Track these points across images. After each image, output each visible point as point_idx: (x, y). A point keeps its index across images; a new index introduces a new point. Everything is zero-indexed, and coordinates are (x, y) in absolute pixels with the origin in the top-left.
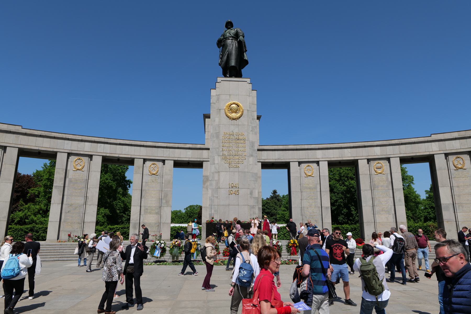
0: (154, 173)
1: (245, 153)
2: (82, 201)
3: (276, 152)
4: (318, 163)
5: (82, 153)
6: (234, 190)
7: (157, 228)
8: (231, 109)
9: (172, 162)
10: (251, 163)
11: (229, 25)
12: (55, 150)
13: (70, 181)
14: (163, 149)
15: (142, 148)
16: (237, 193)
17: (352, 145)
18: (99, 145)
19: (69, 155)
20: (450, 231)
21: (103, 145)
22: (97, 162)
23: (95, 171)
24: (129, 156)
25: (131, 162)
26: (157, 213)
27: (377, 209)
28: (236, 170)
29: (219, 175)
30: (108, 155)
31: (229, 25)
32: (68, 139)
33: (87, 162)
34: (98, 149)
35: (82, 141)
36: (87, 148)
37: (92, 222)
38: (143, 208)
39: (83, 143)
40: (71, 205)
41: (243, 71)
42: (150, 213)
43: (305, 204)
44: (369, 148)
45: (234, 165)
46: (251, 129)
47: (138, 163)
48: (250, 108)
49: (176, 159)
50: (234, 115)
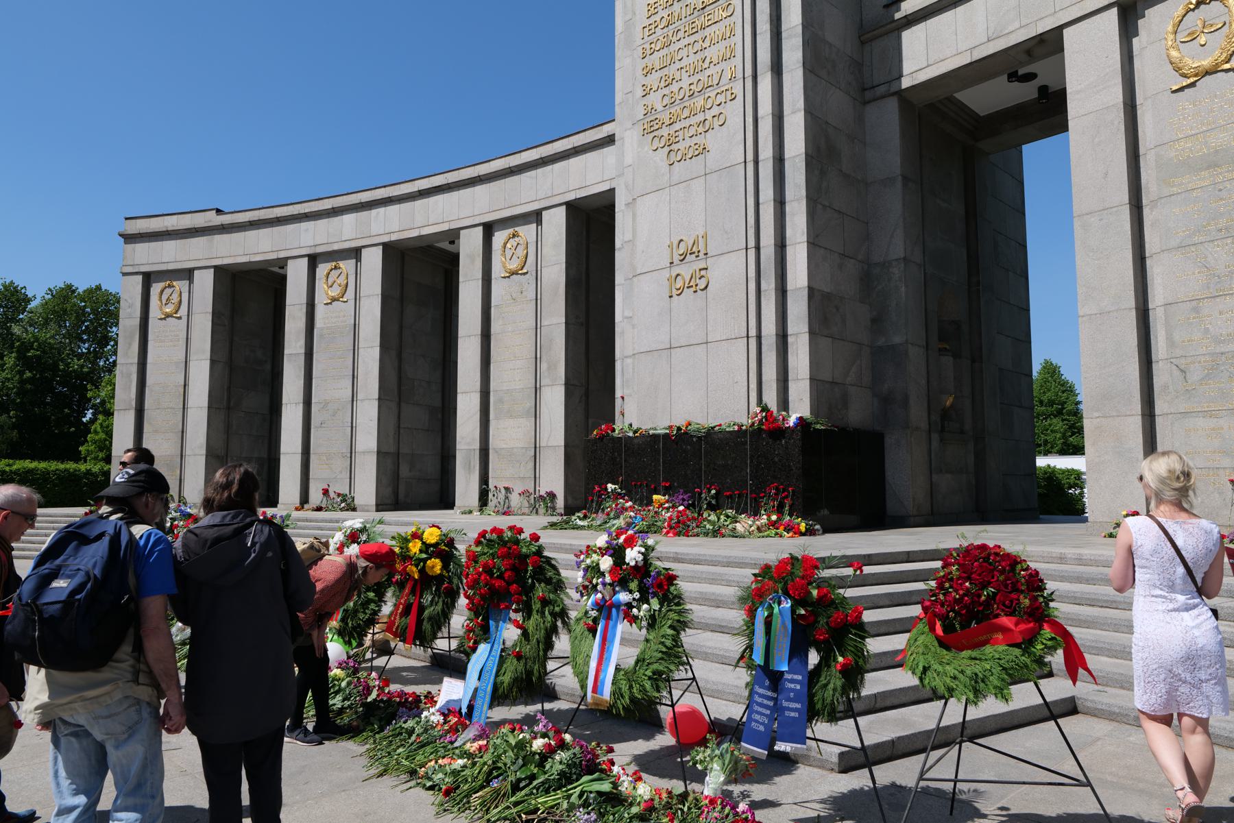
0: (513, 266)
6: (686, 271)
9: (561, 213)
14: (533, 173)
16: (698, 285)
24: (445, 227)
28: (696, 165)
29: (634, 216)
30: (394, 237)
40: (326, 403)
45: (689, 142)
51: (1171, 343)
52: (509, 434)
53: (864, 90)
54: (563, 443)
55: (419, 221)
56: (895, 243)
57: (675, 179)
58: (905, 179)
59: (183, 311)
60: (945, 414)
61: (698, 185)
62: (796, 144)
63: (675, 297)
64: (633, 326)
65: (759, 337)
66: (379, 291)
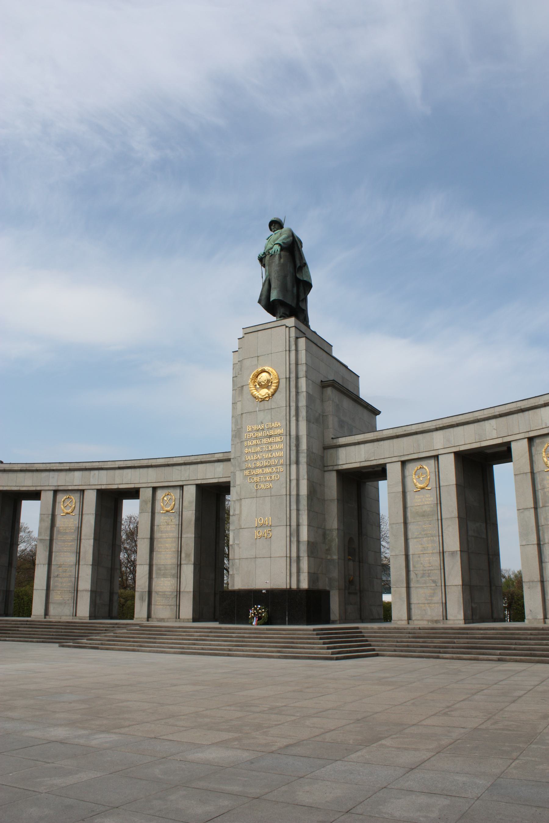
0: (169, 509)
1: (281, 461)
2: (72, 559)
3: (362, 446)
4: (436, 457)
5: (70, 488)
7: (175, 599)
8: (259, 384)
10: (294, 476)
12: (38, 488)
13: (59, 532)
15: (150, 470)
17: (497, 411)
18: (93, 472)
19: (56, 492)
21: (96, 472)
22: (91, 498)
23: (88, 514)
24: (132, 486)
25: (380, 472)
26: (173, 576)
29: (241, 506)
30: (103, 487)
32: (53, 470)
33: (78, 500)
34: (91, 479)
35: (70, 470)
36: (76, 480)
37: (86, 591)
38: (154, 568)
39: (71, 474)
40: (60, 566)
42: (164, 576)
44: (531, 412)
46: (293, 412)
47: (394, 470)
49: (199, 482)
50: (264, 392)
51: (414, 567)
52: (164, 584)
53: (324, 466)
54: (192, 590)
56: (333, 522)
57: (258, 495)
58: (338, 500)
60: (351, 582)
61: (268, 499)
62: (304, 491)
63: (258, 540)
64: (240, 548)
65: (290, 557)
66: (94, 512)
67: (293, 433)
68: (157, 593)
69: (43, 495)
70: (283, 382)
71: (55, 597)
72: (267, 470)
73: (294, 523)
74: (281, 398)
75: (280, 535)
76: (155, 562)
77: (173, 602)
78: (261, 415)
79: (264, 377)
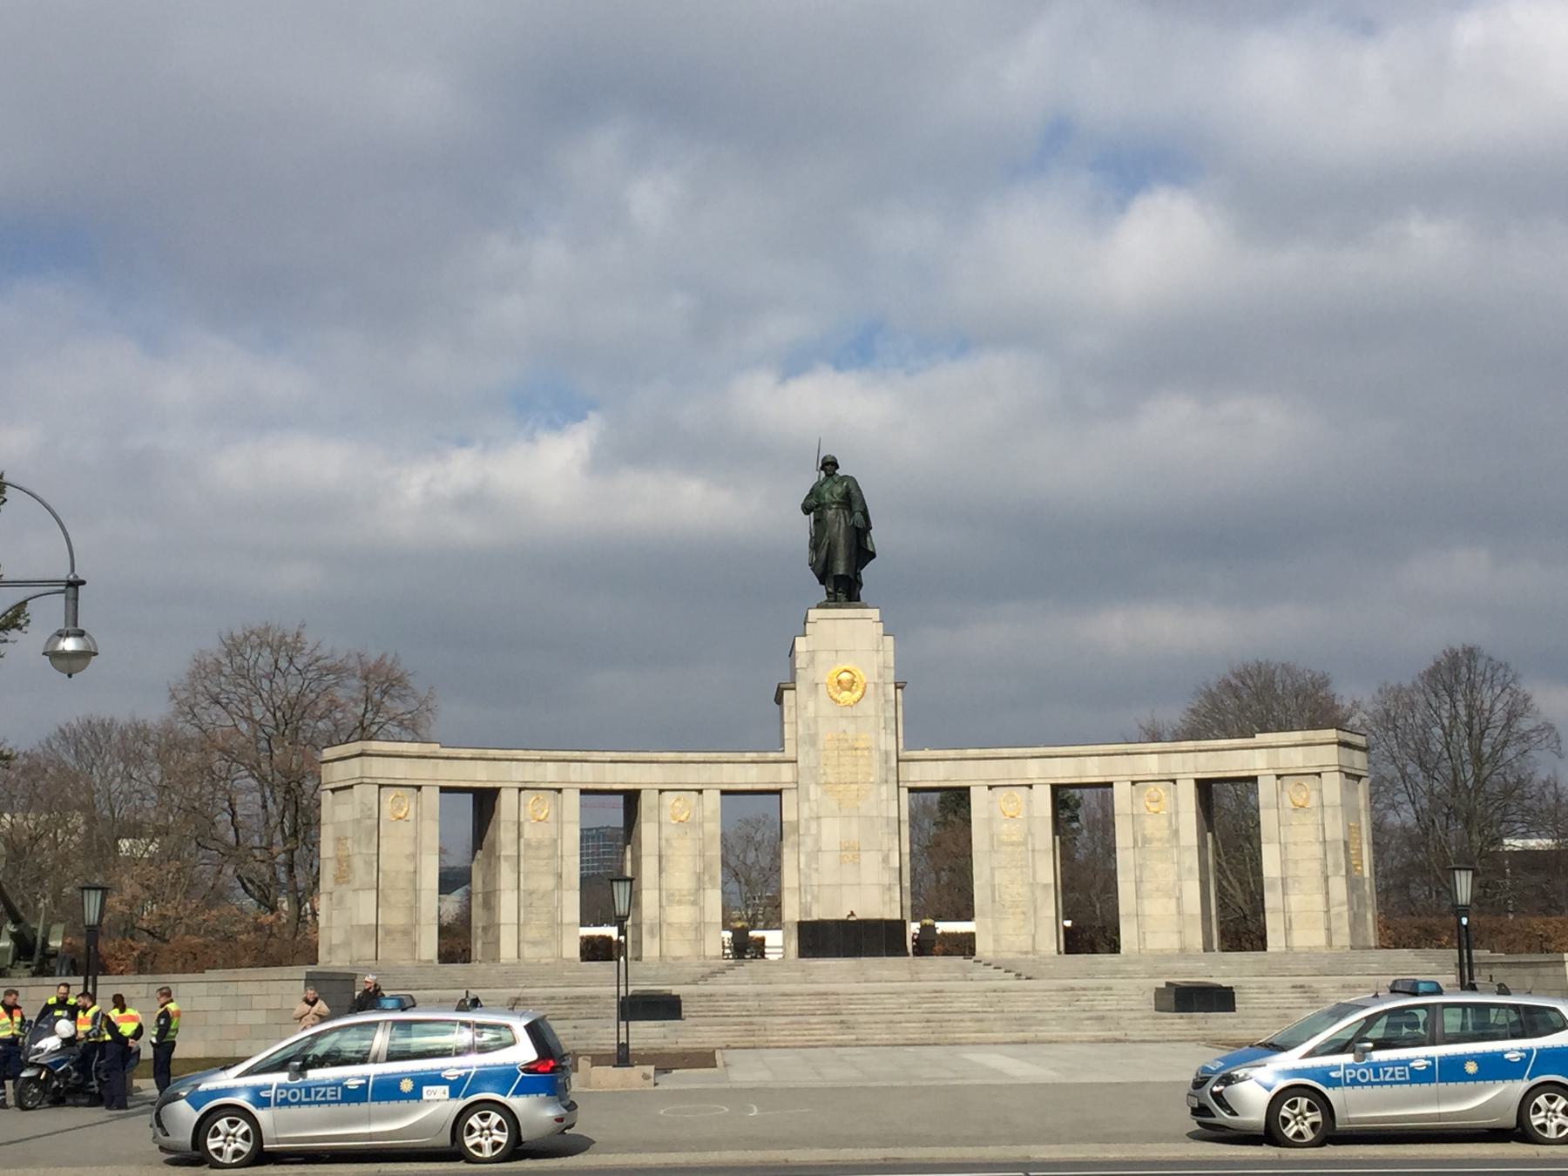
2: (548, 883)
4: (1030, 786)
10: (884, 796)
11: (829, 465)
13: (528, 845)
19: (520, 790)
20: (1274, 930)
26: (694, 903)
27: (1147, 887)
29: (819, 825)
30: (590, 787)
31: (829, 465)
41: (867, 573)
42: (680, 902)
43: (999, 877)
48: (880, 676)
49: (725, 787)
50: (846, 696)
55: (609, 778)
59: (411, 816)
67: (883, 748)
68: (669, 924)
69: (503, 793)
70: (870, 687)
71: (531, 934)
72: (855, 787)
73: (885, 848)
74: (869, 706)
75: (871, 860)
76: (664, 886)
77: (691, 935)
78: (843, 724)
79: (845, 677)
